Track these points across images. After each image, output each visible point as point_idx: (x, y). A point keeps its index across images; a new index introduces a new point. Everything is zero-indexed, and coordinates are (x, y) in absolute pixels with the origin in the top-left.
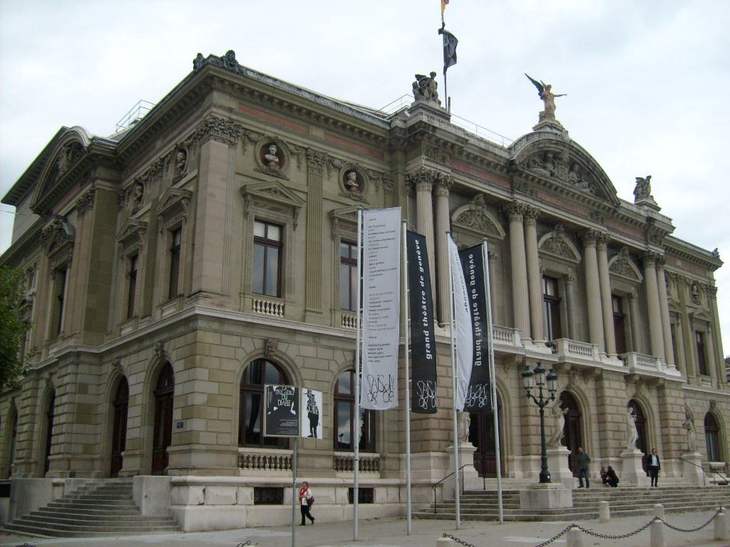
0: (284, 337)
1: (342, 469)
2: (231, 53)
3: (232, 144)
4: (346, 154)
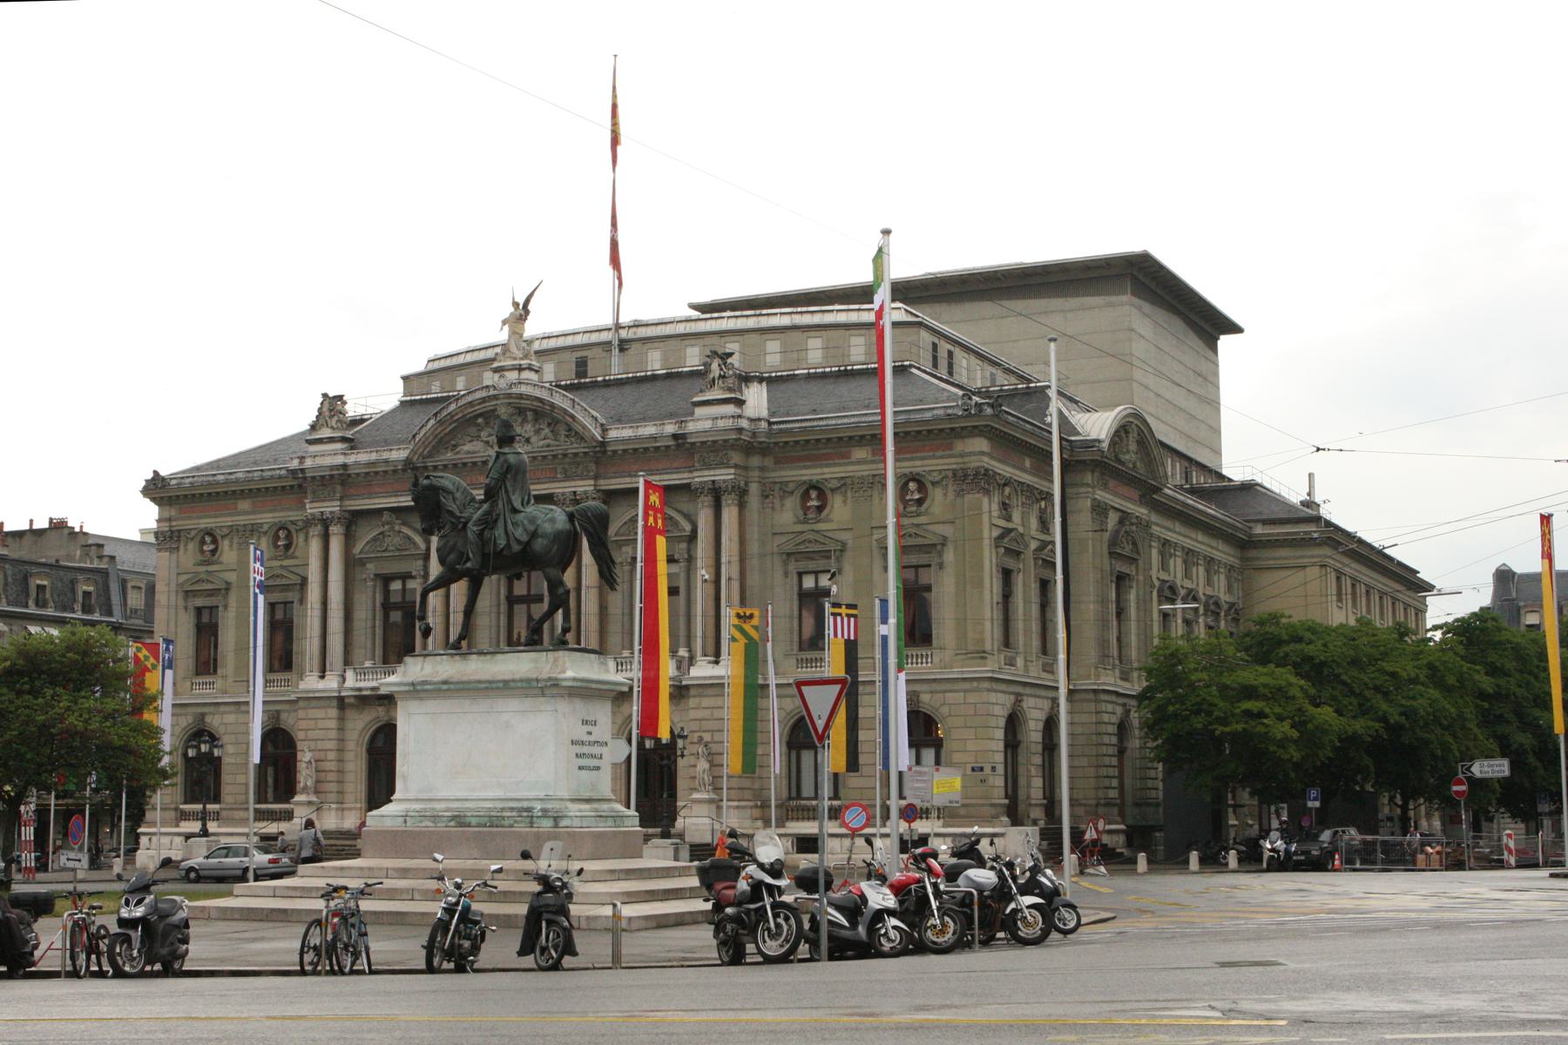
0: (211, 709)
2: (156, 473)
3: (171, 550)
4: (271, 515)
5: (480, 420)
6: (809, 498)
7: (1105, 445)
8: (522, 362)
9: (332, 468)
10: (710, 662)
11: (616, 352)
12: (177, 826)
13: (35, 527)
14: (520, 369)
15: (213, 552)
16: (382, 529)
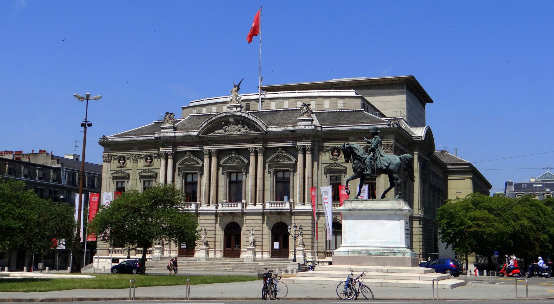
1: (138, 253)
5: (223, 123)
6: (334, 152)
7: (423, 138)
8: (238, 105)
9: (170, 137)
10: (302, 204)
11: (260, 102)
12: (108, 255)
13: (34, 153)
14: (237, 107)
15: (124, 163)
16: (187, 157)
